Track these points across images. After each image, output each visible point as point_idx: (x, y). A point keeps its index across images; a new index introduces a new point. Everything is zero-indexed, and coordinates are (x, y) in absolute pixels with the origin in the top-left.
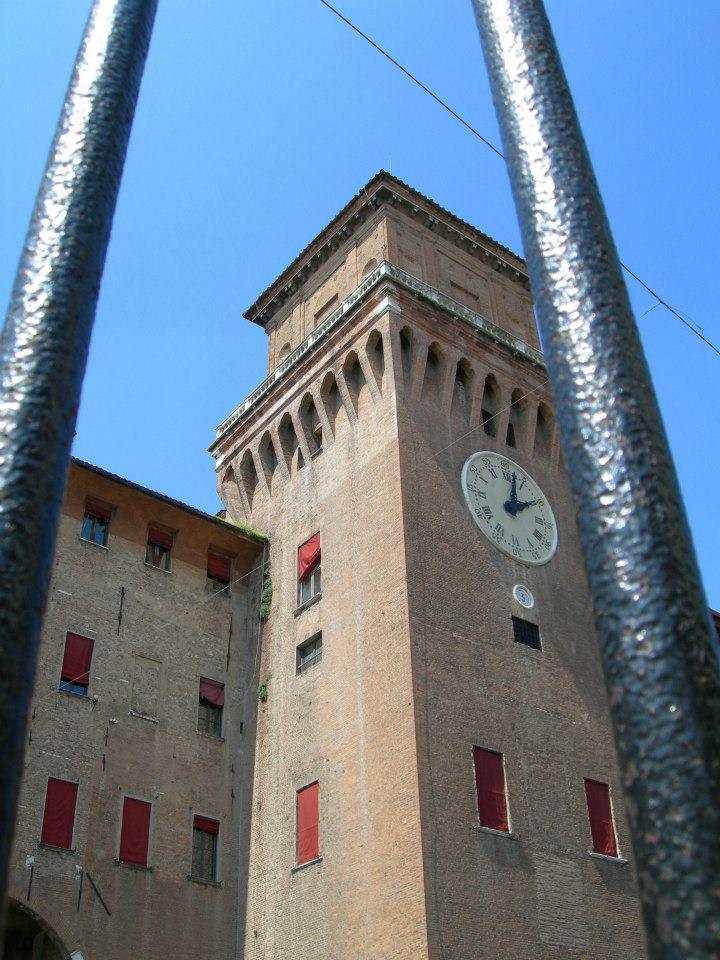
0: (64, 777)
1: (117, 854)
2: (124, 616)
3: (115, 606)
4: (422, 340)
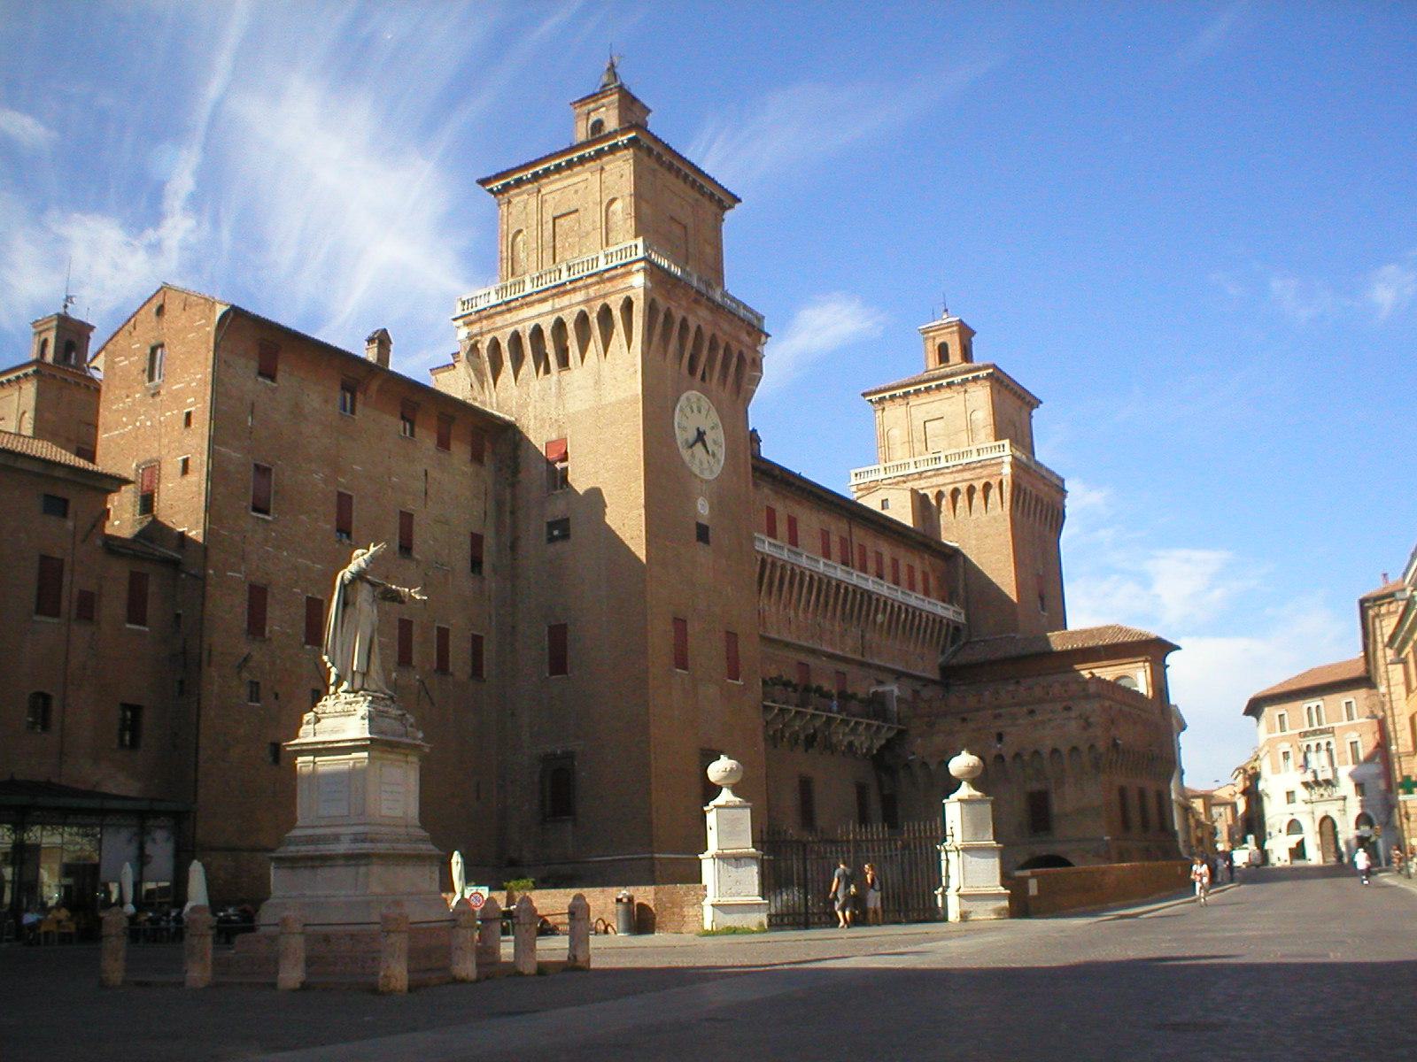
0: (406, 617)
1: (435, 665)
2: (429, 493)
3: (420, 485)
4: (662, 304)
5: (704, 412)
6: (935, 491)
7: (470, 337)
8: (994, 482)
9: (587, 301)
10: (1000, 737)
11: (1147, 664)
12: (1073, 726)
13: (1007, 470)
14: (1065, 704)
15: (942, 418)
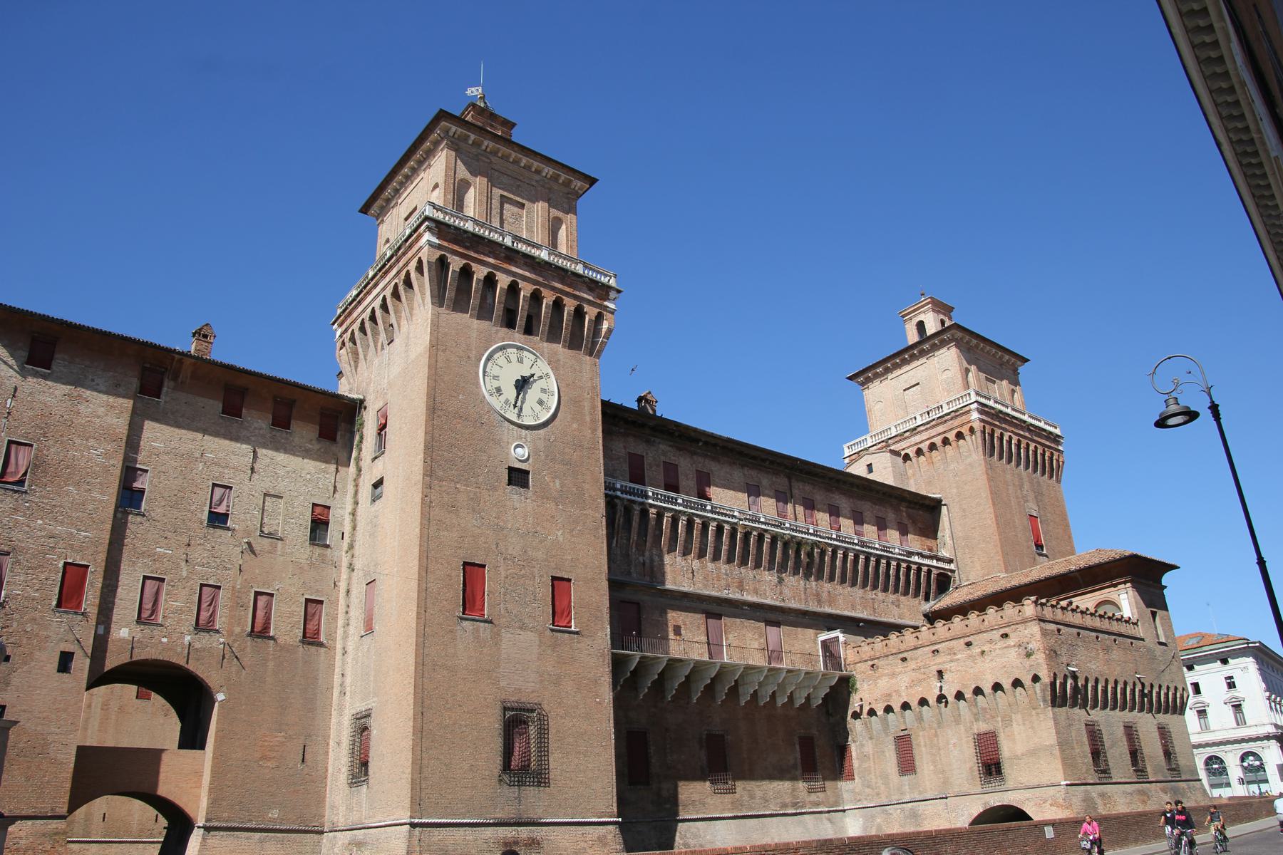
0: (211, 582)
5: (527, 363)
6: (915, 448)
7: (341, 336)
8: (965, 430)
9: (399, 272)
10: (940, 673)
11: (1129, 585)
12: (1013, 653)
13: (975, 415)
14: (1002, 631)
15: (918, 384)
